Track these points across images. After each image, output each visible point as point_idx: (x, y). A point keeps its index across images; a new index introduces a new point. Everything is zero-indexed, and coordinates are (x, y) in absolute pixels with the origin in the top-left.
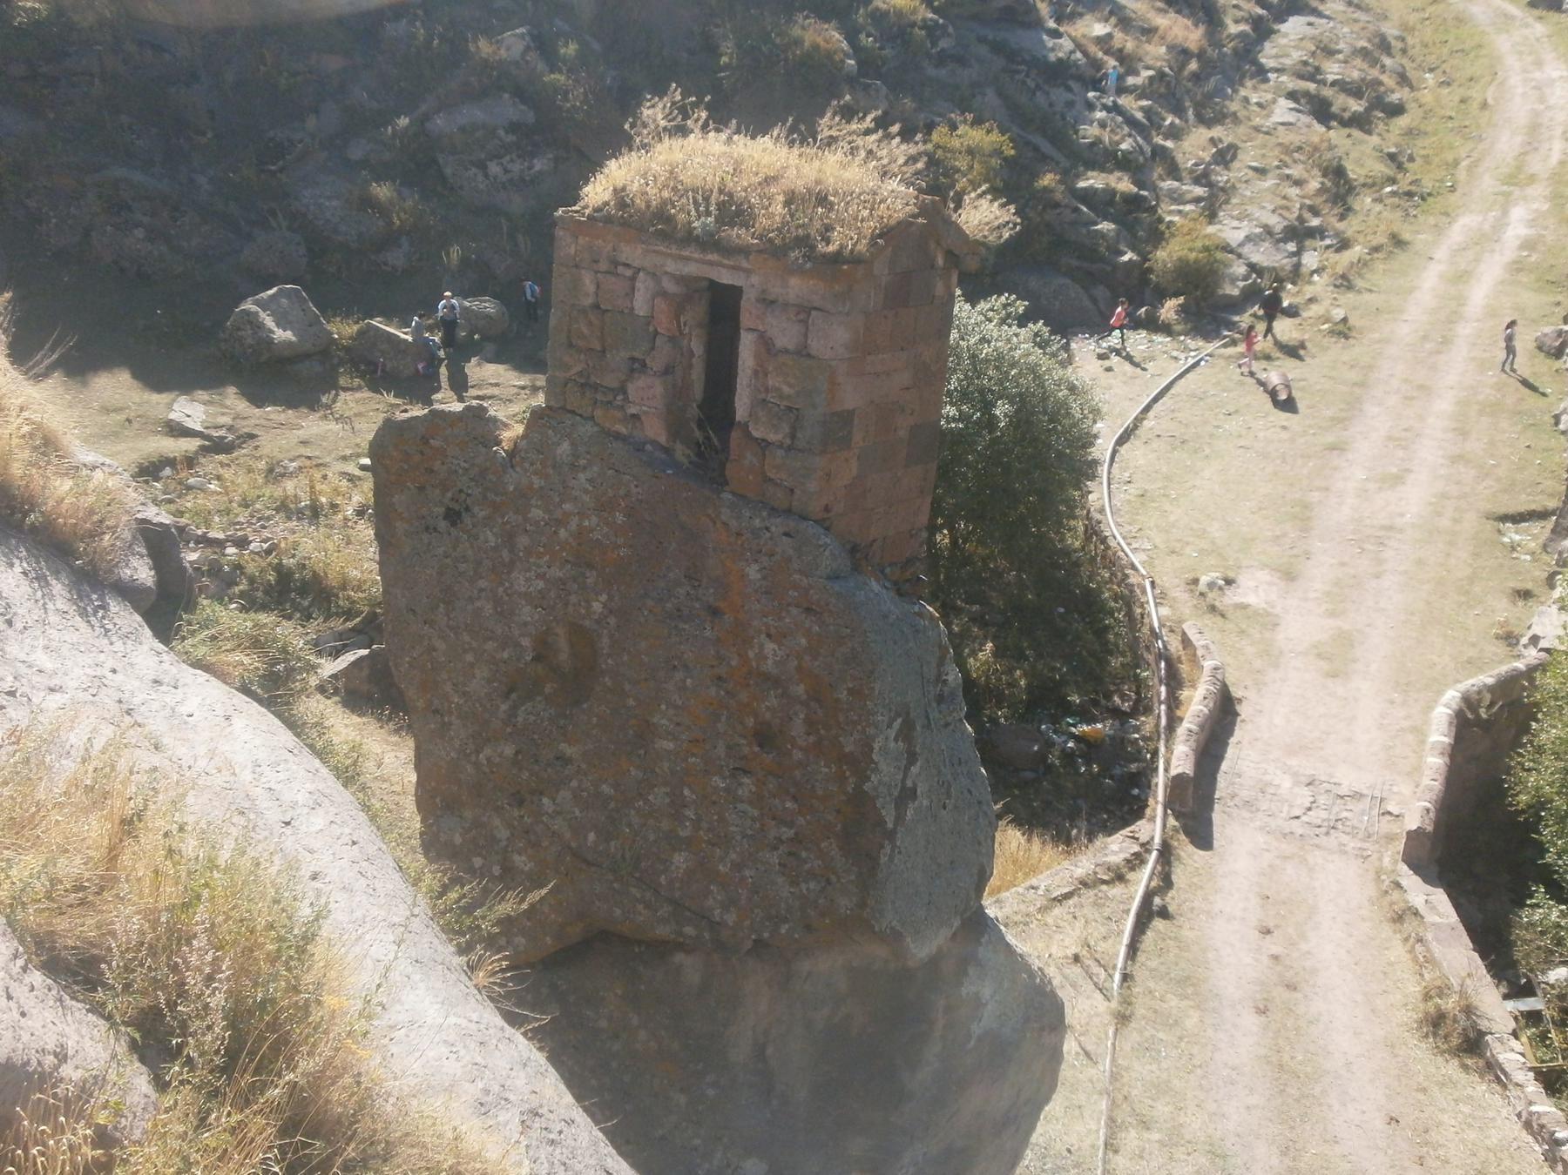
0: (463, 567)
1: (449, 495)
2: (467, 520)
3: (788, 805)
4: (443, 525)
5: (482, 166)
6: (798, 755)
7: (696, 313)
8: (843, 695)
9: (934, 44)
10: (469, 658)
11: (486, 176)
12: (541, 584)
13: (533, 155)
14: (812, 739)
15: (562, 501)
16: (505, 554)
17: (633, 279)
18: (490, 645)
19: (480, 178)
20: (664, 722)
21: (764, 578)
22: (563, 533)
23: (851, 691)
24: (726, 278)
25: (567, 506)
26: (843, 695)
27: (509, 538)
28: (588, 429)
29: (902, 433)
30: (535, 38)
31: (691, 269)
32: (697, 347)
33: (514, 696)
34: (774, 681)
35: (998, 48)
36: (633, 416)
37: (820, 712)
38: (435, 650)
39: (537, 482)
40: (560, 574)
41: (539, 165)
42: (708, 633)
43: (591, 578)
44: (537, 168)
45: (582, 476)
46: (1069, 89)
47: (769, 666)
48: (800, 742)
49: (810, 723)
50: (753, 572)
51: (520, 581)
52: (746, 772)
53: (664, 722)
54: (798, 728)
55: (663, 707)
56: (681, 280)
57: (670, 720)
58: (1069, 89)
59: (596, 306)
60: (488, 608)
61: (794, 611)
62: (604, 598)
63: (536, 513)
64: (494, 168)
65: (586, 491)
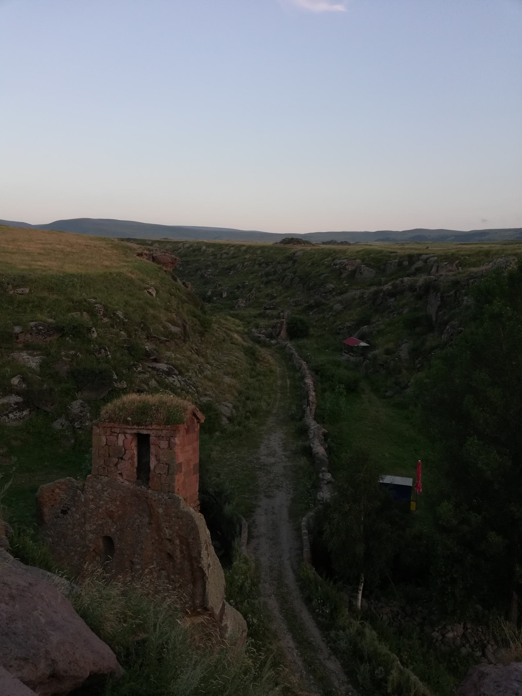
0: (69, 526)
1: (62, 506)
2: (69, 512)
3: (177, 576)
4: (61, 515)
5: (7, 415)
6: (178, 561)
7: (134, 444)
8: (191, 540)
9: (137, 369)
10: (73, 554)
11: (9, 418)
12: (95, 527)
13: (23, 410)
14: (182, 555)
15: (100, 501)
16: (83, 520)
17: (117, 436)
18: (79, 549)
19: (7, 419)
20: (137, 560)
21: (164, 512)
22: (100, 510)
23: (193, 539)
24: (145, 432)
25: (101, 502)
26: (191, 540)
27: (84, 514)
28: (105, 479)
29: (192, 467)
30: (21, 378)
31: (135, 431)
32: (135, 452)
33: (87, 563)
34: (170, 540)
35: (154, 368)
36: (119, 474)
37: (184, 547)
38: (61, 553)
39: (91, 497)
40: (100, 522)
41: (25, 413)
42: (148, 531)
43: (110, 521)
44: (24, 414)
45: (106, 493)
46: (173, 377)
47: (168, 536)
48: (179, 557)
49: (182, 551)
50: (160, 511)
51: (88, 527)
52: (163, 570)
53: (137, 560)
54: (178, 553)
55: (136, 556)
56: (131, 434)
57: (138, 559)
58: (173, 377)
59: (107, 444)
60: (77, 537)
61: (174, 519)
62: (115, 527)
63: (92, 506)
64: (11, 415)
65: (108, 497)
